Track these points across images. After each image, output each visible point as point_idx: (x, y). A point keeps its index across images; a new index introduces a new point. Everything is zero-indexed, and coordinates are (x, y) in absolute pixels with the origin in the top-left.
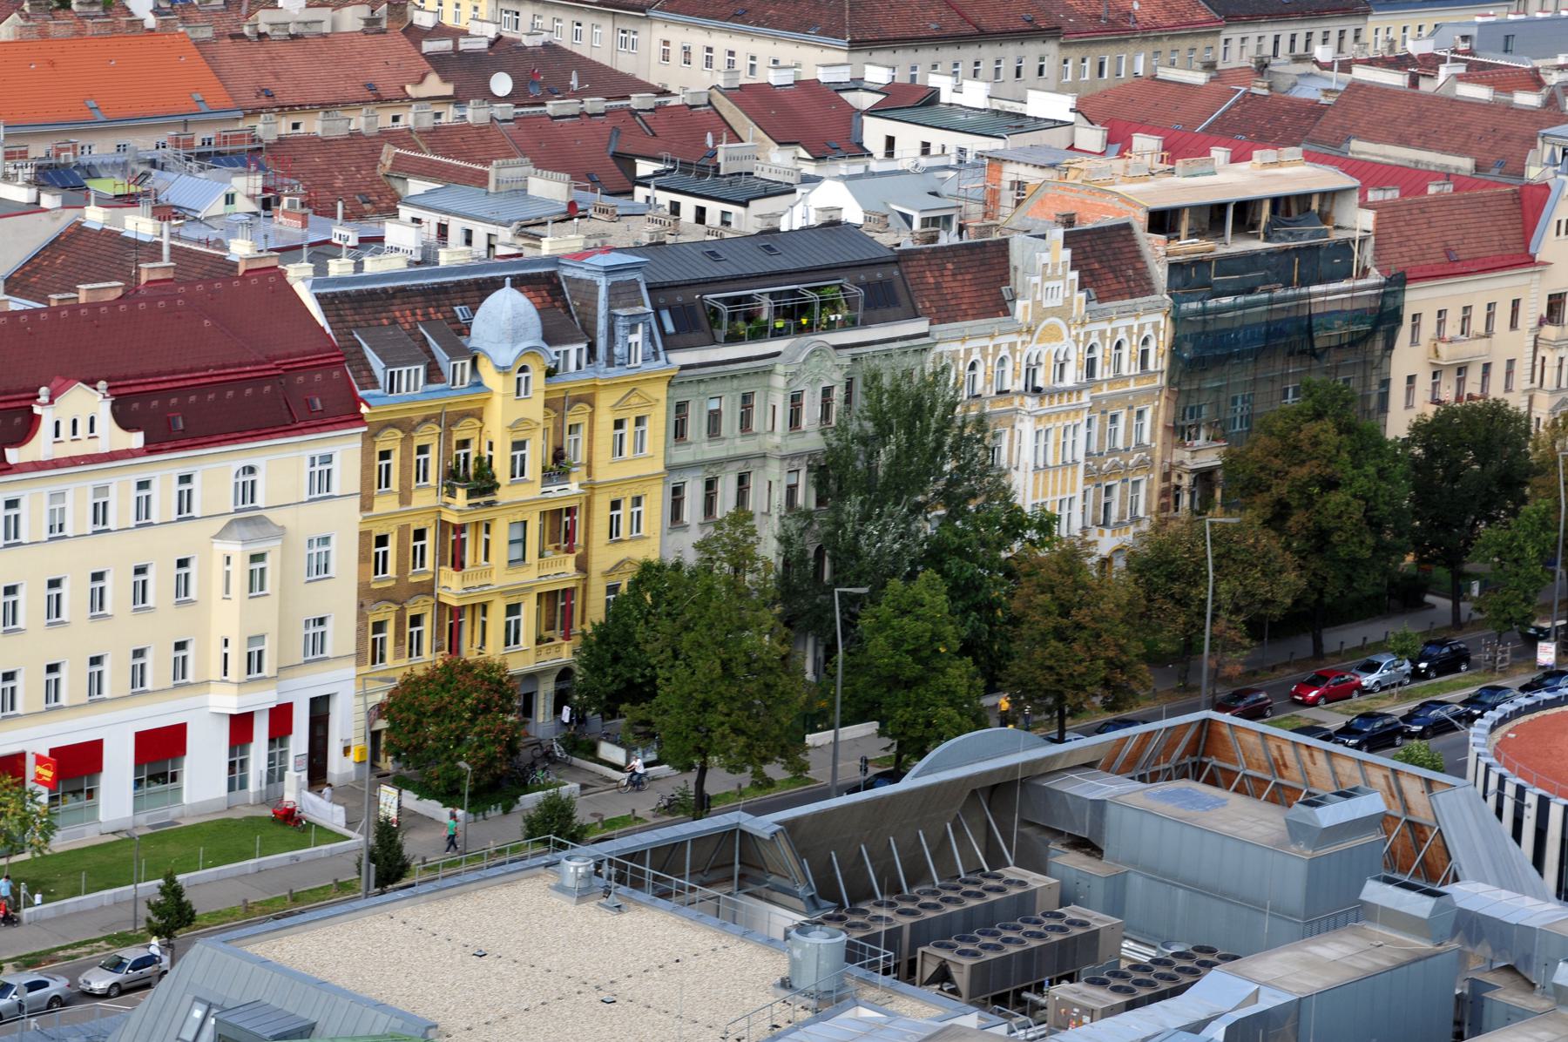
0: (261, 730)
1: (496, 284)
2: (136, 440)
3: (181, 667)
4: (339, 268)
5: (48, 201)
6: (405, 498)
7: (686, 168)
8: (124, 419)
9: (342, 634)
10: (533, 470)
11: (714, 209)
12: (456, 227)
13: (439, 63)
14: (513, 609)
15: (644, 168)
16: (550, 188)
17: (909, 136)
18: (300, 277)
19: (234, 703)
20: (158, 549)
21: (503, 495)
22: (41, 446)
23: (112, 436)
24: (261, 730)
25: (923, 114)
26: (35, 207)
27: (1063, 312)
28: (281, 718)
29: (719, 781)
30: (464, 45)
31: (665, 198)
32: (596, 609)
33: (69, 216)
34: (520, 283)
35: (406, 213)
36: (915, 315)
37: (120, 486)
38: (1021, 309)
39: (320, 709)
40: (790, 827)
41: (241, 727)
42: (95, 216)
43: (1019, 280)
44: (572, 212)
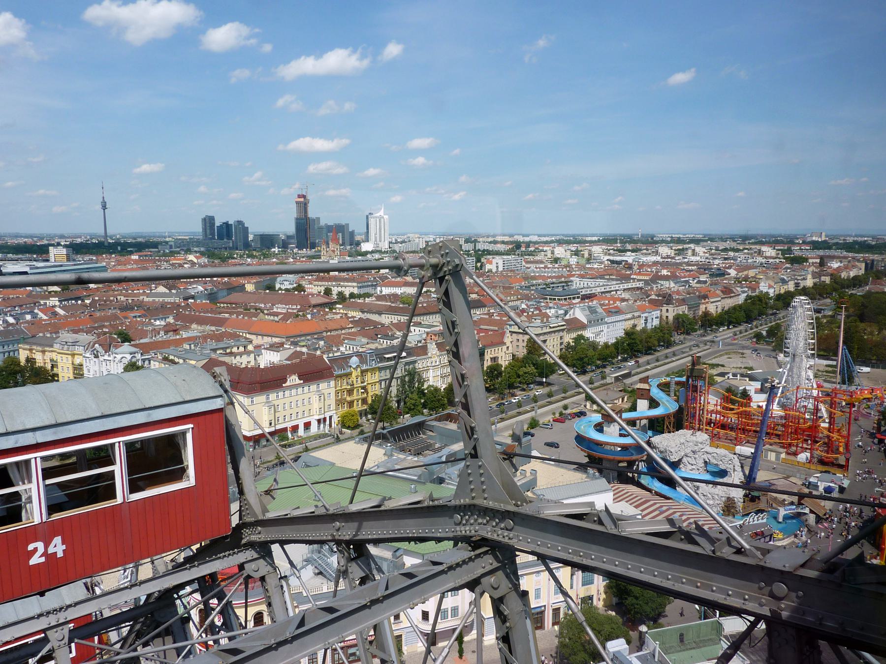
0: (322, 421)
1: (353, 356)
2: (302, 382)
3: (310, 413)
4: (331, 355)
5: (292, 347)
6: (341, 387)
7: (385, 335)
8: (300, 379)
9: (333, 407)
10: (359, 382)
11: (389, 341)
12: (351, 347)
13: (351, 321)
14: (358, 402)
15: (379, 336)
16: (365, 340)
17: (417, 329)
18: (325, 357)
19: (318, 417)
20: (306, 396)
21: (355, 386)
22: (288, 384)
23: (298, 381)
24: (322, 421)
25: (419, 326)
26: (290, 348)
27: (436, 354)
28: (325, 419)
29: (386, 425)
30: (355, 319)
31: (382, 340)
32: (370, 401)
33: (295, 349)
34: (356, 356)
35: (344, 345)
36: (414, 356)
37: (300, 390)
38: (429, 355)
39: (331, 418)
40: (388, 432)
41: (319, 421)
42: (298, 349)
43: (429, 350)
44: (368, 344)
